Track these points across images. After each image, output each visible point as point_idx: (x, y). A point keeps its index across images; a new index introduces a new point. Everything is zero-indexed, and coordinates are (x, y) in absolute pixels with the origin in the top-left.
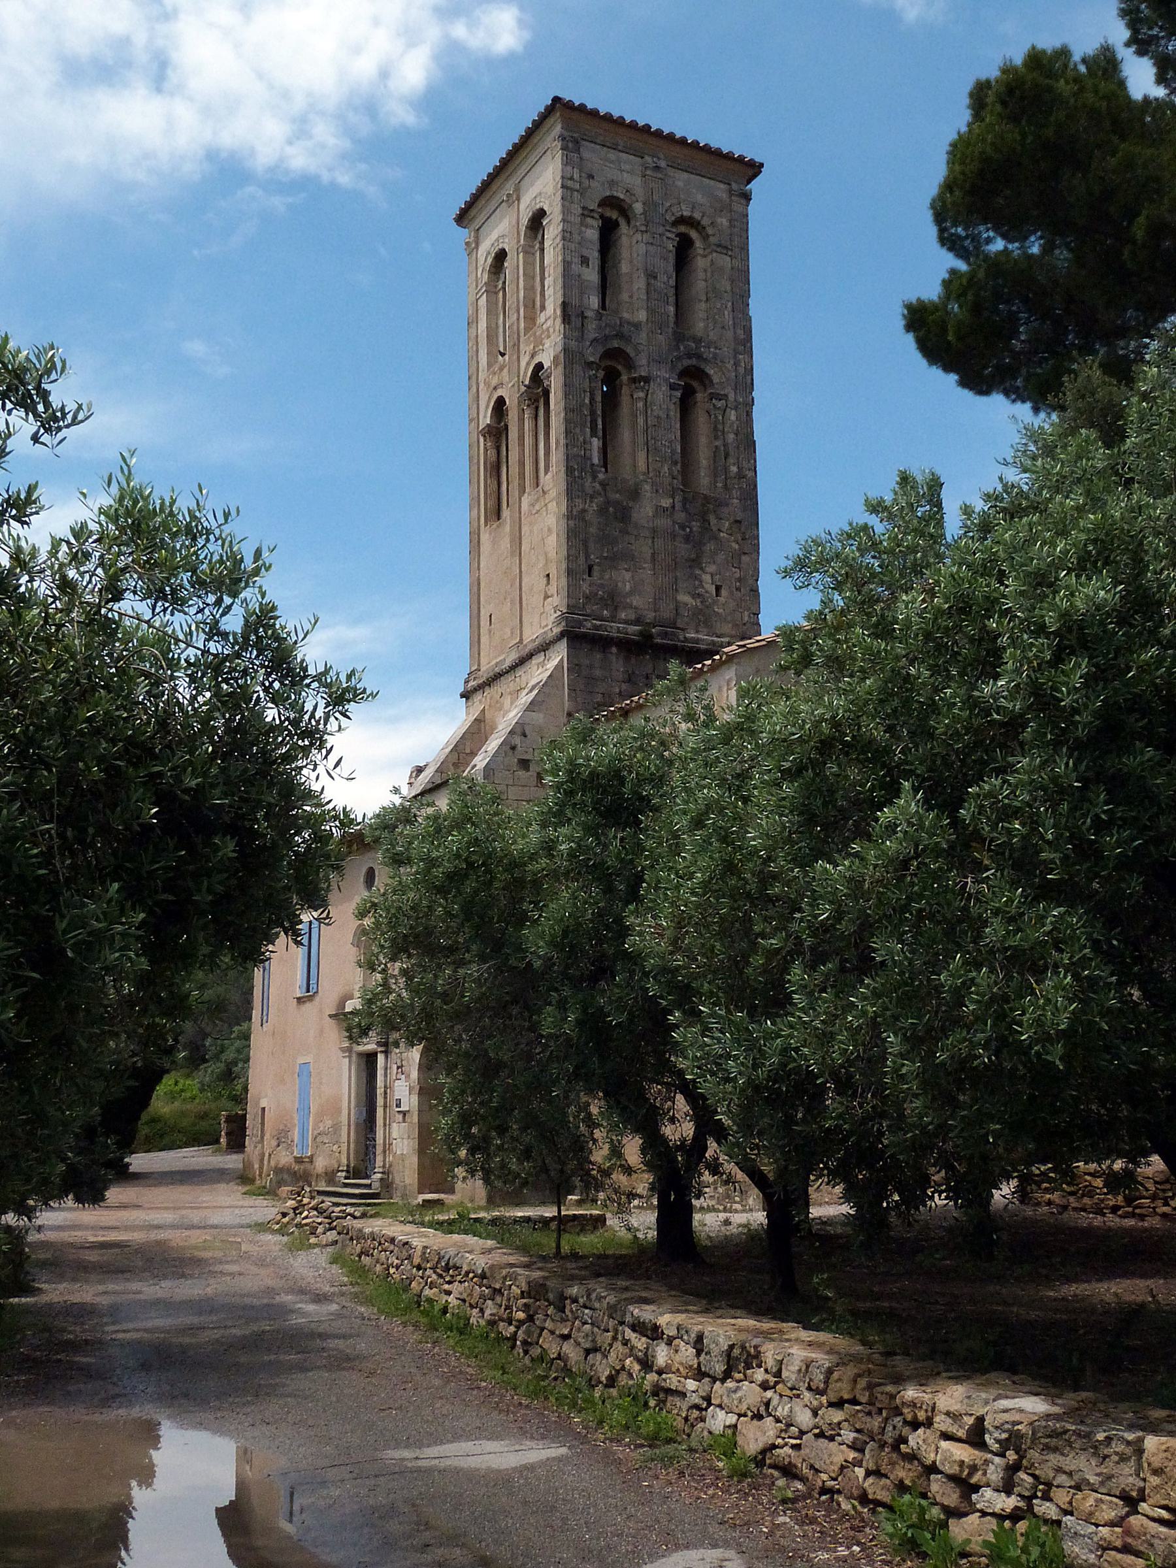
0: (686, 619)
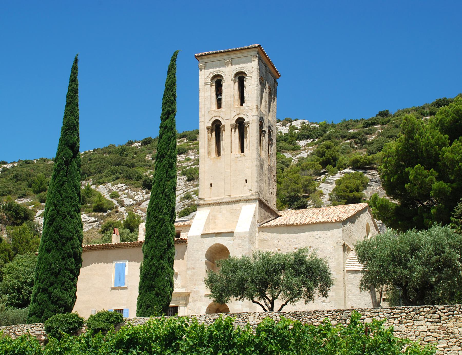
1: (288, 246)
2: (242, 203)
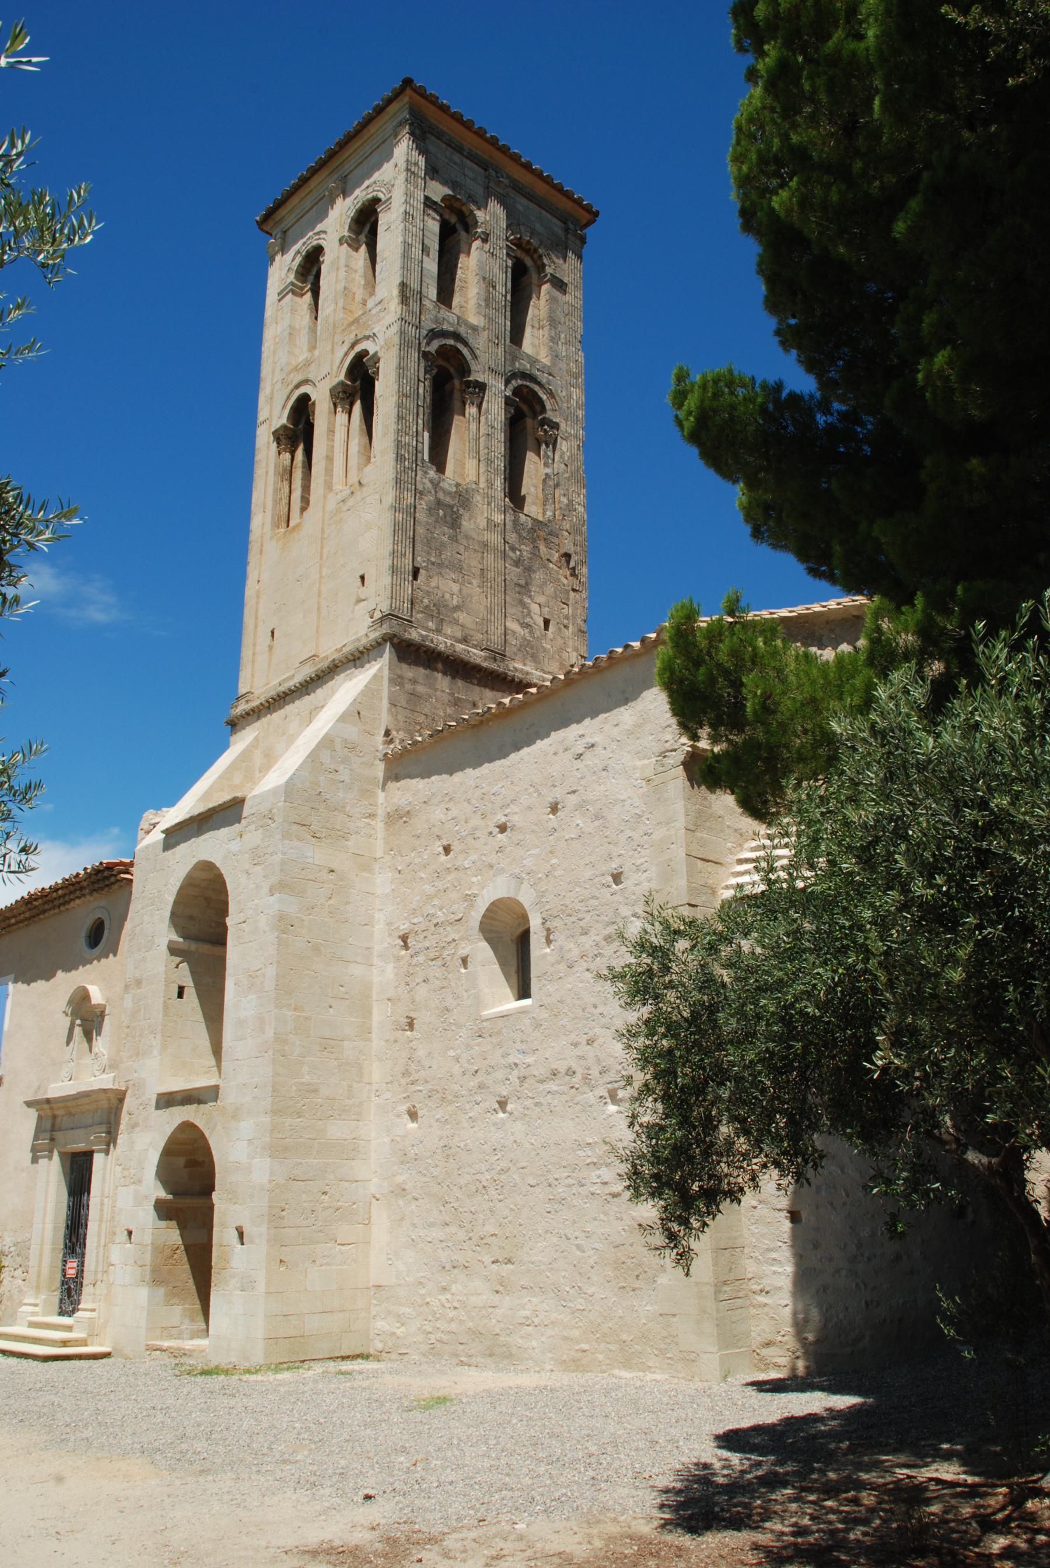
0: (515, 649)
1: (476, 821)
2: (342, 675)
